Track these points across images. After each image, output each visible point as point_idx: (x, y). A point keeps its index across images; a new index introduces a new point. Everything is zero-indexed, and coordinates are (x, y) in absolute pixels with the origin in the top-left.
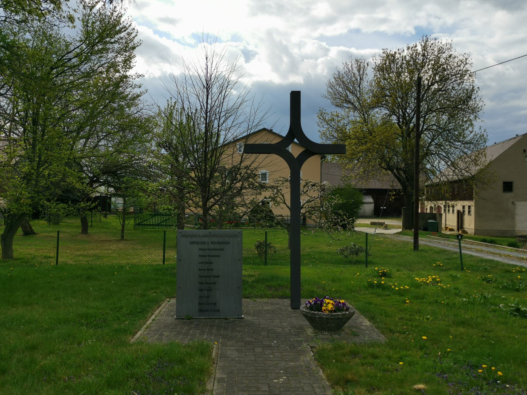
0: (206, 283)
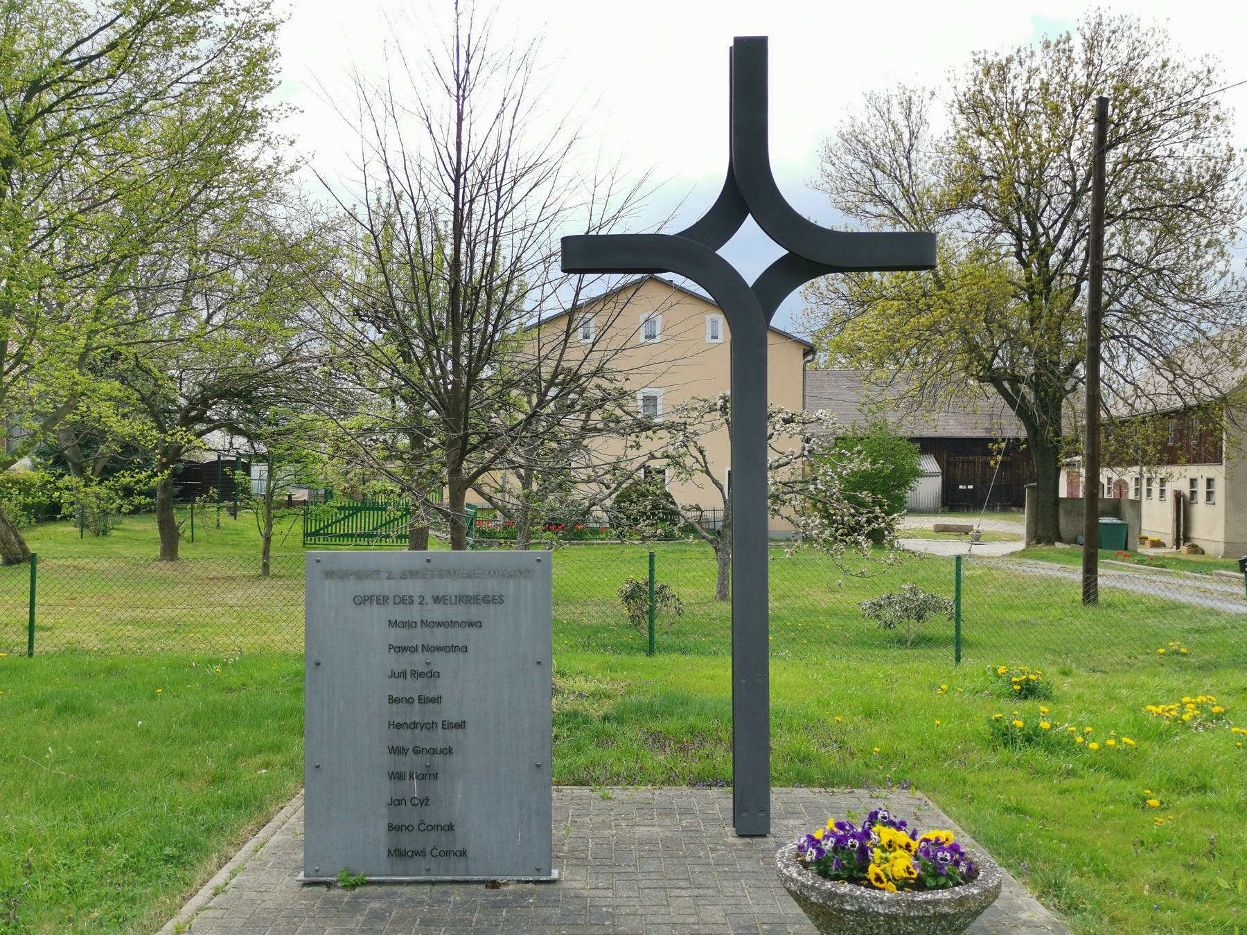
0: (417, 751)
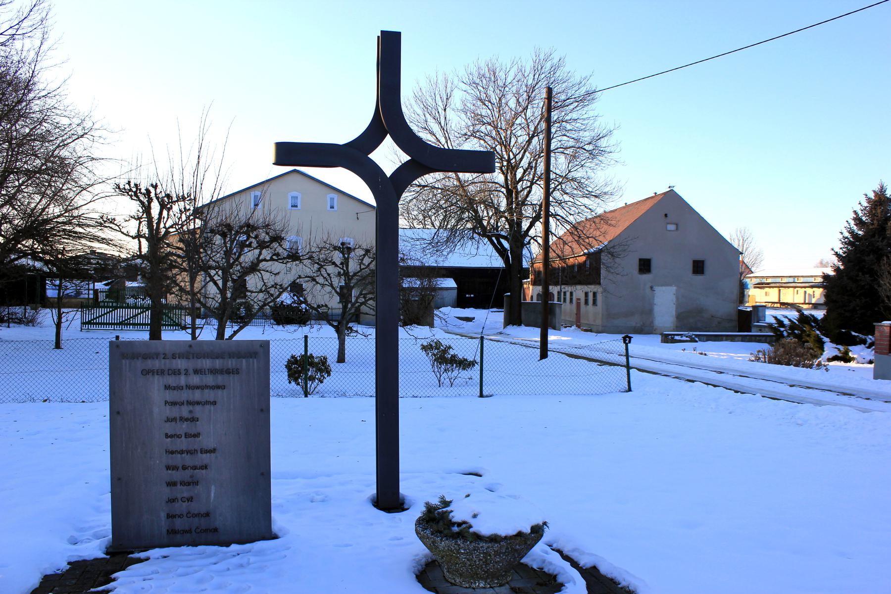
0: (184, 468)
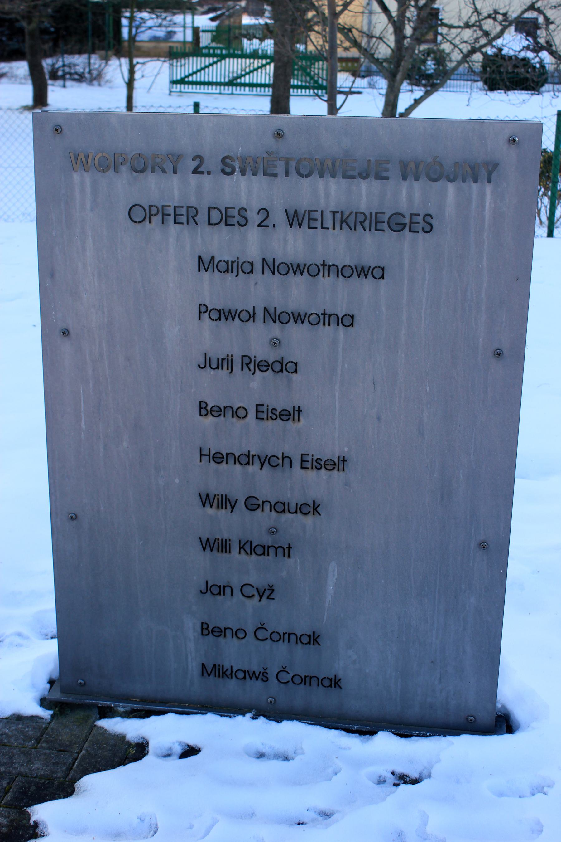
0: (253, 504)
